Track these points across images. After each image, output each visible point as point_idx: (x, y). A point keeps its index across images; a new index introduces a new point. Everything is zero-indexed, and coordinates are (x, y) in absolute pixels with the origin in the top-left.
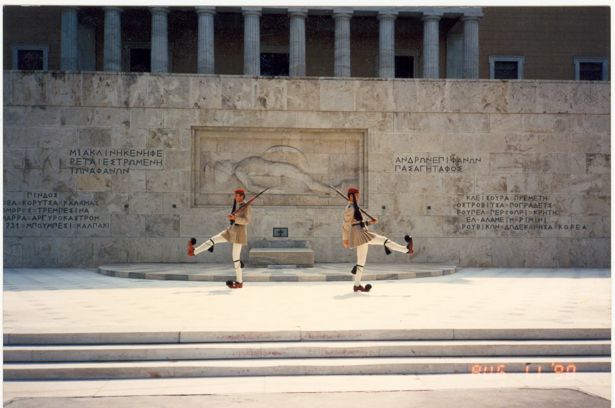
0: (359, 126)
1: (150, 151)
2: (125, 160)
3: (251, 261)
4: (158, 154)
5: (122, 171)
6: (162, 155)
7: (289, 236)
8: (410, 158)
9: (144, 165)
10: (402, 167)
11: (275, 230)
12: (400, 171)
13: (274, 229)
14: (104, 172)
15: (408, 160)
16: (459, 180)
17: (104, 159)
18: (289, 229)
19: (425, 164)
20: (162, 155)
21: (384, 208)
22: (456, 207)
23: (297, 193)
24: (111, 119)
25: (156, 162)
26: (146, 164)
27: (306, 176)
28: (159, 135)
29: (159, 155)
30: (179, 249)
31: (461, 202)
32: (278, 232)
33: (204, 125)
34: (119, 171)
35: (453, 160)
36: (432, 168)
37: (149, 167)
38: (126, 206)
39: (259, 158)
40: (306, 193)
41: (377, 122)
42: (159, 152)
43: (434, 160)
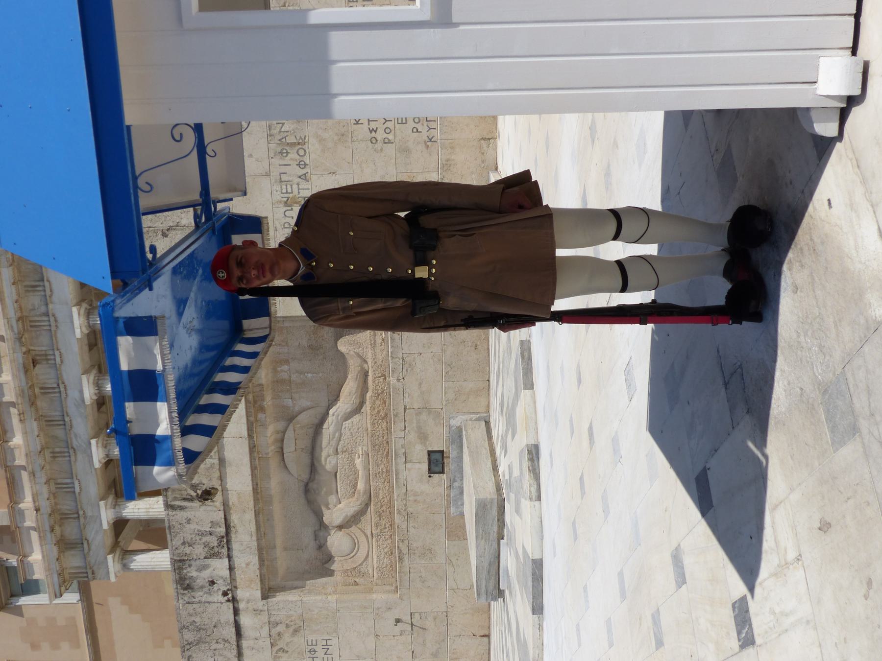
13: (431, 471)
16: (321, 140)
18: (430, 449)
22: (378, 146)
28: (281, 644)
29: (314, 643)
31: (369, 136)
35: (282, 154)
42: (310, 643)
43: (287, 193)
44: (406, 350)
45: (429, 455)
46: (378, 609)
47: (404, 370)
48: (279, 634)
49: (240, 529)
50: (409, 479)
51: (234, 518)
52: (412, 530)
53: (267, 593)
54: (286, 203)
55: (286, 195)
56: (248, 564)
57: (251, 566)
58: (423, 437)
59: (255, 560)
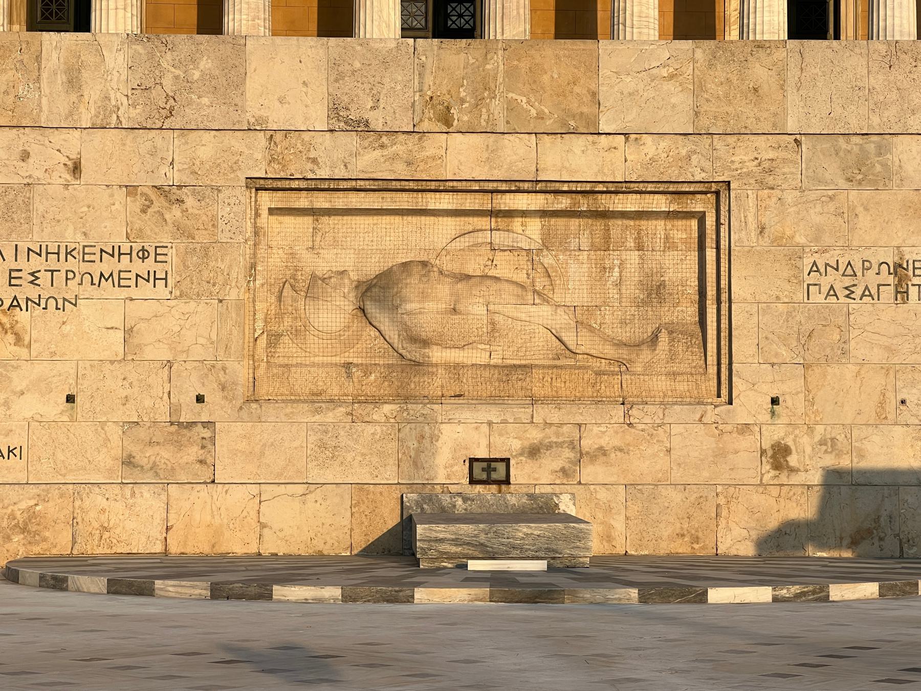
0: (703, 175)
1: (137, 247)
2: (67, 271)
3: (422, 549)
4: (156, 254)
5: (60, 302)
6: (168, 259)
7: (512, 480)
8: (849, 263)
9: (119, 286)
10: (825, 289)
11: (475, 464)
12: (820, 299)
13: (472, 461)
14: (11, 305)
15: (842, 268)
17: (11, 271)
18: (512, 462)
19: (891, 279)
20: (168, 259)
21: (775, 401)
23: (537, 362)
24: (31, 160)
25: (152, 278)
26: (123, 283)
27: (560, 311)
28: (159, 203)
29: (159, 258)
30: (213, 517)
32: (483, 470)
33: (282, 175)
34: (52, 302)
36: (911, 289)
37: (133, 292)
38: (70, 399)
39: (424, 264)
40: (557, 363)
41: (756, 162)
42: (159, 251)
43: (914, 268)
44: (676, 429)
45: (502, 460)
46: (224, 369)
47: (643, 426)
48: (180, 201)
49: (378, 153)
50: (460, 428)
51: (400, 147)
52: (370, 429)
53: (257, 185)
54: (900, 266)
55: (911, 267)
56: (314, 161)
57: (310, 166)
58: (534, 452)
59: (324, 173)
